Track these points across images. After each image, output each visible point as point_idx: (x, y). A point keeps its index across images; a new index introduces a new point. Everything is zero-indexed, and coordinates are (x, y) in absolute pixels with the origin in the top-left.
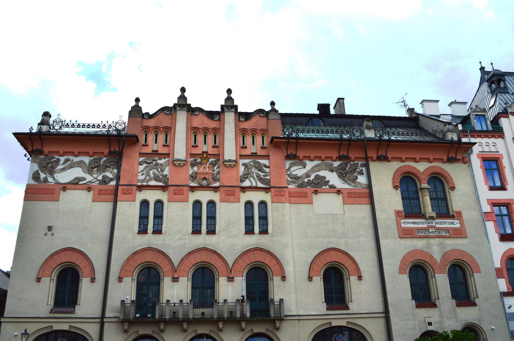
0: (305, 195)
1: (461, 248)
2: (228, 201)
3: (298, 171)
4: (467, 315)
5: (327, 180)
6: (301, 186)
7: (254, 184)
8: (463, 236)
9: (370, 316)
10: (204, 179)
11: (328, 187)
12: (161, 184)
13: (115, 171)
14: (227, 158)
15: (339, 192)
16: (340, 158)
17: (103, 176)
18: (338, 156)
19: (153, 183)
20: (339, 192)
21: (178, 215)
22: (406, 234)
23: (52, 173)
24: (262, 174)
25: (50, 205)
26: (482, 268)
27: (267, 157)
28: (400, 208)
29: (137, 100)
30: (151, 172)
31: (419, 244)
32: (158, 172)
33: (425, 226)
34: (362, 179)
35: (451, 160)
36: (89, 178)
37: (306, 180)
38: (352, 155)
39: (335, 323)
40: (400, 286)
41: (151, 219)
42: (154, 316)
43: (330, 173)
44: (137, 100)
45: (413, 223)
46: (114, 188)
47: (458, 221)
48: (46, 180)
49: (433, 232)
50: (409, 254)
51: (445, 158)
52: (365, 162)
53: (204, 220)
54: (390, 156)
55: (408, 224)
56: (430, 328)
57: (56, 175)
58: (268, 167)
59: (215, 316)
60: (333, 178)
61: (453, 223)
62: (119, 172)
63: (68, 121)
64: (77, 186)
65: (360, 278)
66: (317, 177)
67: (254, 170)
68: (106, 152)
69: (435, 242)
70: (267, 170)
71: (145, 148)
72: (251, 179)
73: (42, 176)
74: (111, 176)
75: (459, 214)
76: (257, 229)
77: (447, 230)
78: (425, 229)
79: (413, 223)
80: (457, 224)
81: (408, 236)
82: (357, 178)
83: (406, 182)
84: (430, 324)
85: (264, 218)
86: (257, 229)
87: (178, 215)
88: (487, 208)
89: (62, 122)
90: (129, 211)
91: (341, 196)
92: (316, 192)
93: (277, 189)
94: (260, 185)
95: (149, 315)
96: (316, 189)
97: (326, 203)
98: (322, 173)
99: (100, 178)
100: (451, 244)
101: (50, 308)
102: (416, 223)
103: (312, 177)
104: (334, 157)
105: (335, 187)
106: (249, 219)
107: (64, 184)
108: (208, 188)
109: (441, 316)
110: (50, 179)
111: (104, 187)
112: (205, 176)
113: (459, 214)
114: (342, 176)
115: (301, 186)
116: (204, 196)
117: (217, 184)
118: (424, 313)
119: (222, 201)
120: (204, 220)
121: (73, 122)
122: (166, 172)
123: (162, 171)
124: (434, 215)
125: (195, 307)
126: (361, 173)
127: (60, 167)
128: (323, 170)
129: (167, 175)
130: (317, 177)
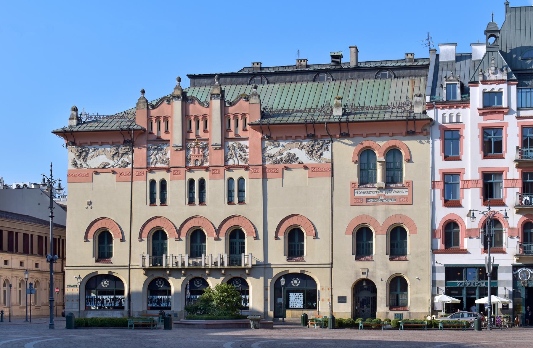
0: (277, 171)
1: (403, 213)
2: (214, 179)
3: (272, 150)
4: (397, 267)
5: (296, 157)
6: (275, 163)
7: (236, 163)
8: (407, 203)
9: (320, 266)
10: (197, 160)
11: (296, 163)
12: (165, 166)
13: (130, 156)
14: (213, 143)
15: (306, 168)
16: (308, 137)
17: (122, 161)
18: (306, 135)
19: (159, 165)
20: (306, 168)
21: (177, 190)
22: (357, 202)
23: (85, 159)
24: (243, 154)
25: (88, 185)
26: (419, 231)
27: (246, 139)
28: (356, 180)
29: (143, 92)
30: (157, 156)
31: (367, 210)
32: (162, 155)
33: (375, 195)
34: (327, 155)
35: (411, 134)
36: (112, 163)
37: (279, 158)
38: (318, 134)
39: (291, 271)
40: (346, 243)
41: (158, 194)
42: (161, 265)
43: (299, 150)
44: (143, 92)
45: (365, 192)
46: (131, 171)
47: (407, 190)
48: (82, 166)
49: (381, 200)
50: (357, 218)
51: (404, 132)
52: (330, 139)
53: (196, 192)
54: (351, 134)
55: (361, 193)
56: (364, 276)
57: (87, 161)
58: (247, 148)
59: (203, 266)
60: (302, 155)
61: (402, 192)
62: (132, 157)
63: (91, 114)
64: (104, 169)
65: (316, 237)
66: (289, 154)
67: (238, 151)
68: (122, 141)
69: (380, 208)
70: (247, 150)
71: (151, 135)
72: (235, 158)
73: (78, 162)
74: (128, 161)
75: (410, 184)
76: (236, 200)
77: (393, 198)
78: (374, 198)
79: (365, 192)
80: (406, 192)
81: (359, 204)
82: (322, 154)
83: (365, 158)
84: (363, 273)
85: (241, 191)
86: (236, 200)
87: (177, 190)
88: (438, 177)
89: (86, 115)
90: (142, 188)
91: (306, 171)
92: (287, 168)
93: (253, 167)
94: (241, 163)
95: (159, 265)
96: (286, 165)
97: (295, 176)
98: (292, 152)
99: (120, 162)
100: (396, 209)
101: (94, 259)
102: (368, 192)
103: (285, 154)
104: (303, 136)
105: (303, 163)
106: (230, 192)
107: (94, 168)
108: (201, 167)
109: (375, 268)
110: (84, 165)
111: (123, 170)
112: (197, 158)
113: (410, 184)
114: (310, 153)
115: (275, 163)
116: (197, 175)
117: (206, 164)
118: (362, 265)
119: (210, 178)
120: (196, 192)
121: (95, 114)
122: (168, 156)
123: (166, 154)
124: (383, 185)
125: (190, 258)
126: (327, 149)
127: (90, 155)
128: (293, 148)
129: (169, 158)
130: (289, 154)
